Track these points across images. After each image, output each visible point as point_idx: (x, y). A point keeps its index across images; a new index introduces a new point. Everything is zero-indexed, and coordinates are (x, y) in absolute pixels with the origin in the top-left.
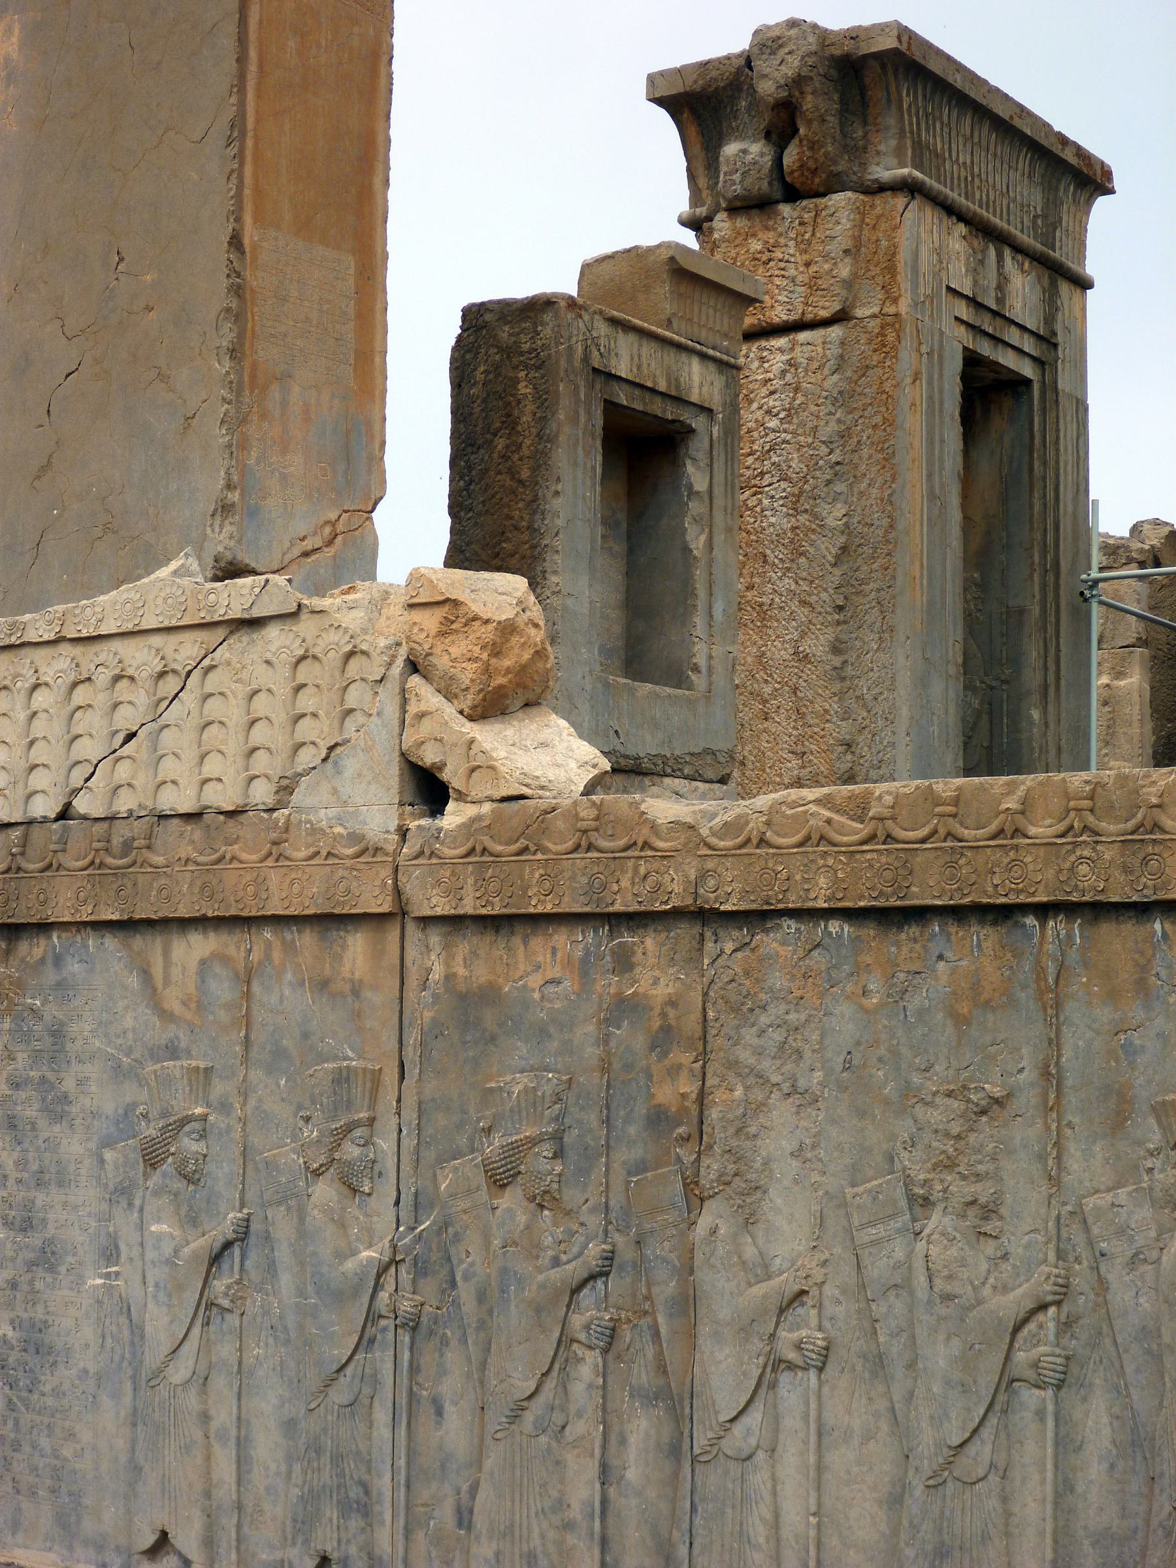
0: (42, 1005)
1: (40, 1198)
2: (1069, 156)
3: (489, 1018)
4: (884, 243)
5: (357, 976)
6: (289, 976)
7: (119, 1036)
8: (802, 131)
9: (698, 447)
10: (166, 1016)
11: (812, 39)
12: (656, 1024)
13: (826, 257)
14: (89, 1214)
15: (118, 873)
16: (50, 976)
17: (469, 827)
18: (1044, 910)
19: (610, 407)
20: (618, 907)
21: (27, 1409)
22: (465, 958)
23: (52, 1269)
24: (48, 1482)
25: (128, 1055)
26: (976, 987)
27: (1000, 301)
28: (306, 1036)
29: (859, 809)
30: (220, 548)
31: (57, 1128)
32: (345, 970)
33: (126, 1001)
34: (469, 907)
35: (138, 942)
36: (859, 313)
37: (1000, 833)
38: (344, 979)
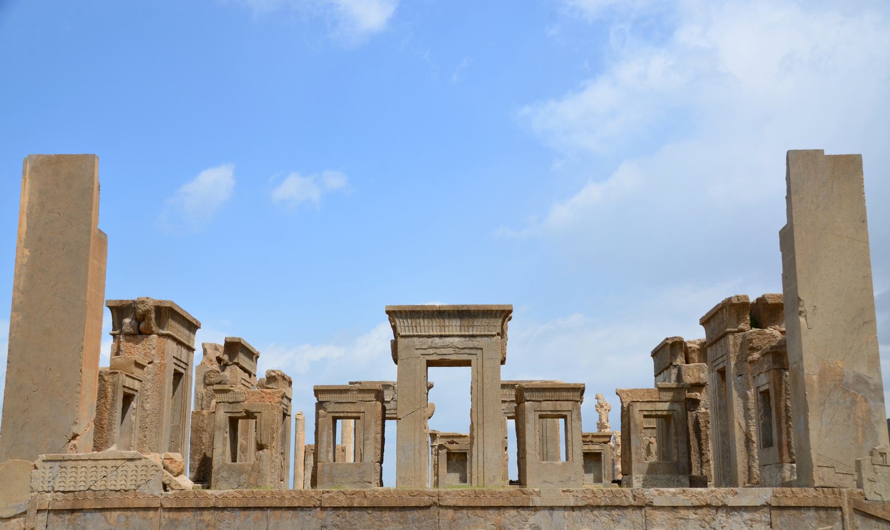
2: (194, 322)
3: (176, 523)
4: (162, 347)
9: (136, 398)
11: (152, 302)
12: (206, 523)
13: (149, 349)
15: (101, 500)
17: (175, 494)
18: (268, 508)
19: (124, 392)
20: (202, 506)
26: (257, 517)
27: (181, 357)
29: (241, 493)
30: (74, 431)
34: (174, 506)
36: (155, 361)
37: (262, 497)
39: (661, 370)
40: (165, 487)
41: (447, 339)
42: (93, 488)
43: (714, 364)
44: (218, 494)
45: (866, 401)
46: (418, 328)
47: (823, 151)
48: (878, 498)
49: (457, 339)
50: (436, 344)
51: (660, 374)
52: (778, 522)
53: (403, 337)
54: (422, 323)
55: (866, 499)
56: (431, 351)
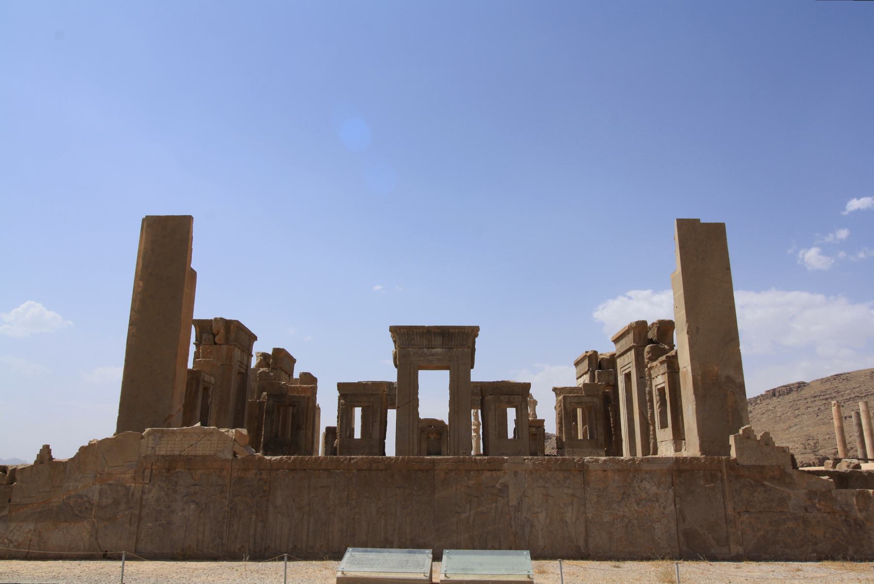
8: (220, 335)
39: (581, 374)
42: (182, 454)
43: (623, 369)
44: (273, 459)
45: (734, 394)
46: (413, 342)
47: (699, 220)
48: (745, 463)
49: (439, 350)
50: (425, 354)
51: (580, 377)
52: (678, 482)
53: (401, 348)
54: (415, 338)
55: (738, 464)
56: (422, 359)
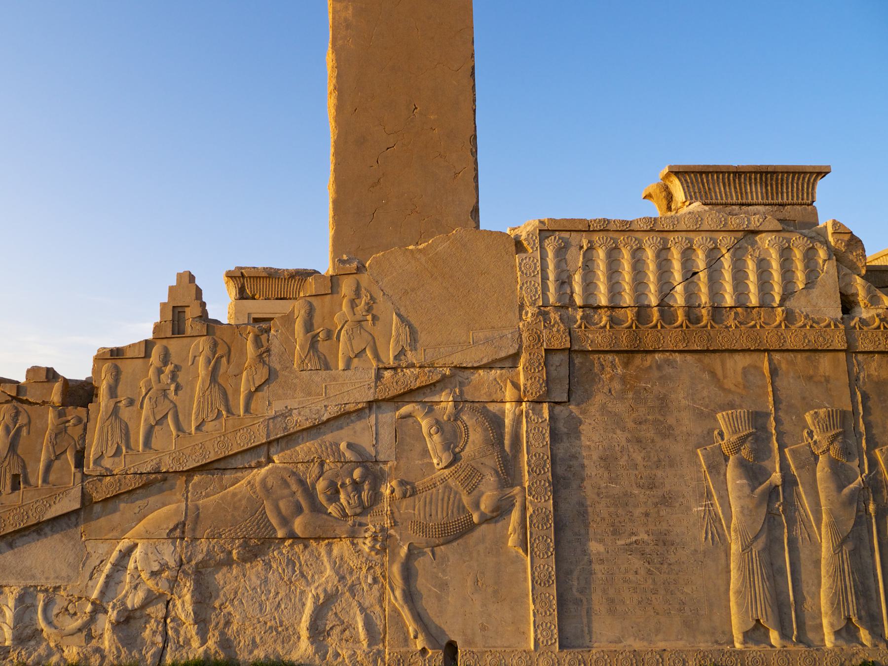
0: (652, 386)
1: (659, 473)
5: (827, 374)
6: (792, 374)
7: (700, 400)
10: (729, 391)
14: (692, 479)
16: (656, 374)
21: (660, 573)
22: (875, 369)
23: (670, 505)
24: (677, 606)
25: (706, 408)
28: (804, 398)
31: (667, 441)
32: (821, 371)
33: (703, 385)
35: (707, 359)
38: (820, 376)
40: (848, 305)
41: (750, 207)
